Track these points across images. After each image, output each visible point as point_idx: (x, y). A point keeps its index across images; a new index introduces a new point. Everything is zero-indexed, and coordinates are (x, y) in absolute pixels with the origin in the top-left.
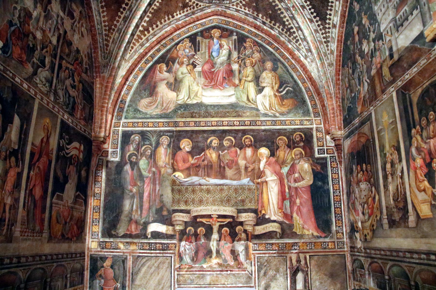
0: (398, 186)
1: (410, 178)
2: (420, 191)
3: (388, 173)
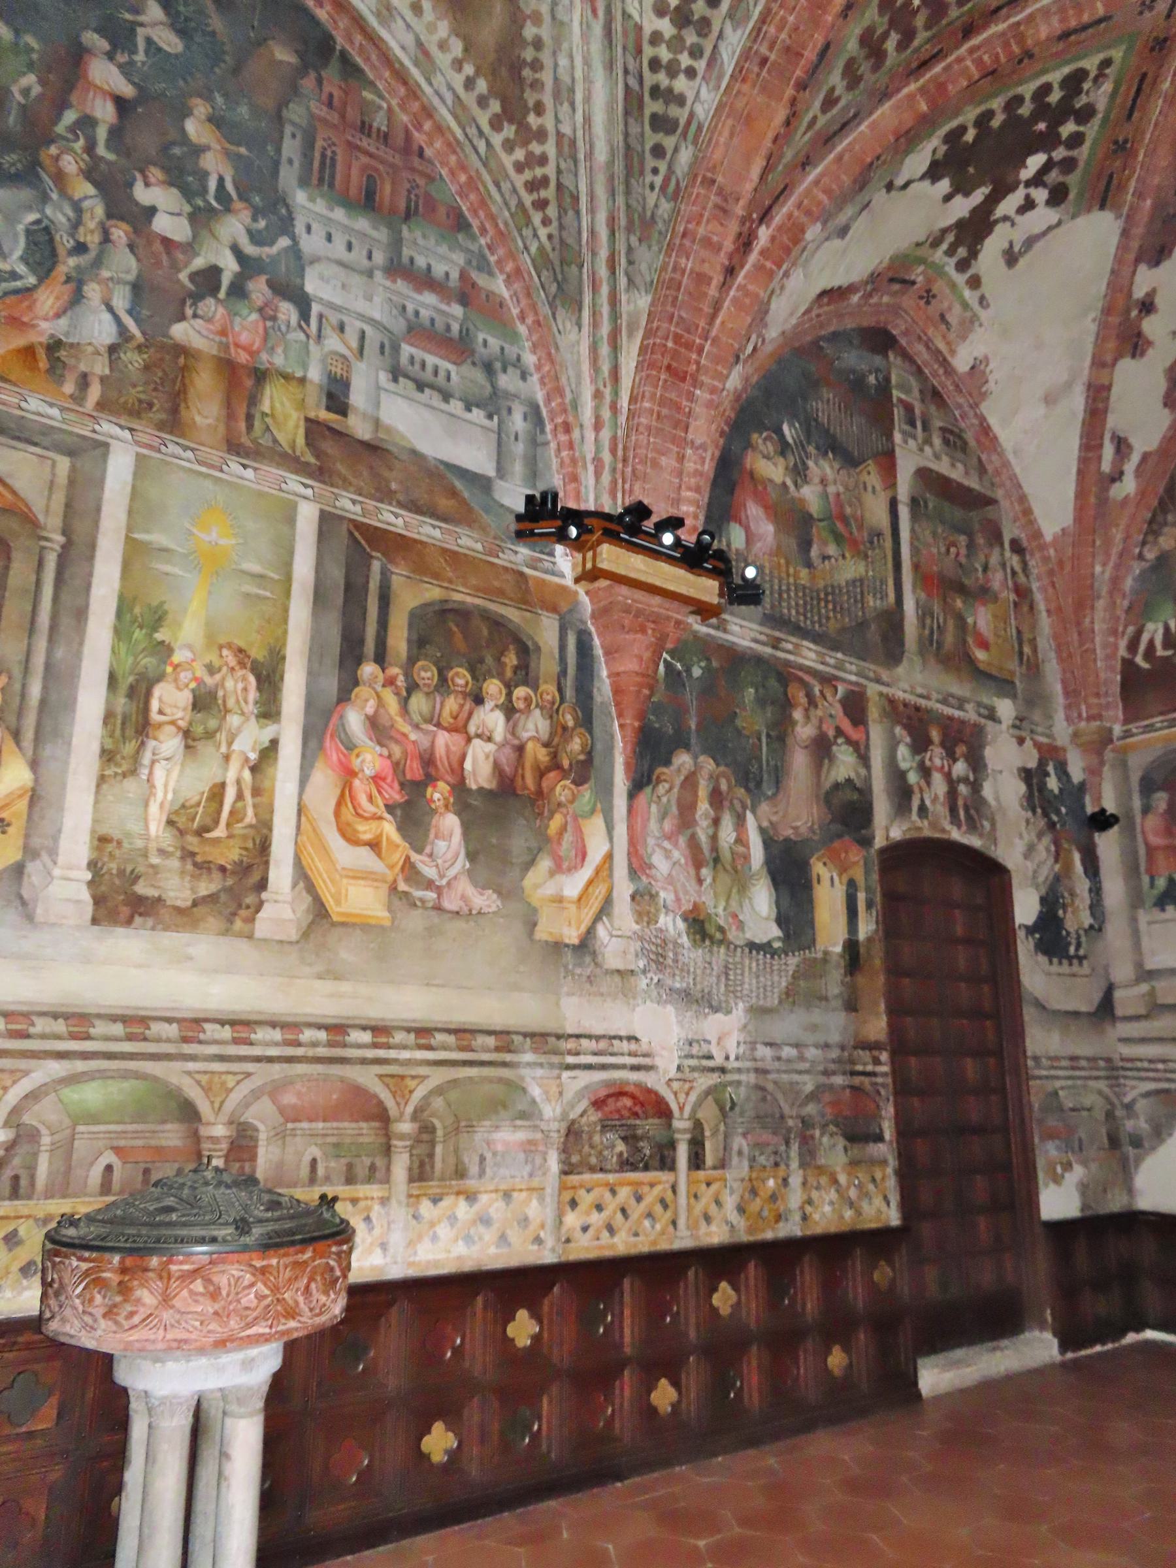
0: (223, 785)
1: (309, 789)
2: (352, 839)
3: (155, 716)
